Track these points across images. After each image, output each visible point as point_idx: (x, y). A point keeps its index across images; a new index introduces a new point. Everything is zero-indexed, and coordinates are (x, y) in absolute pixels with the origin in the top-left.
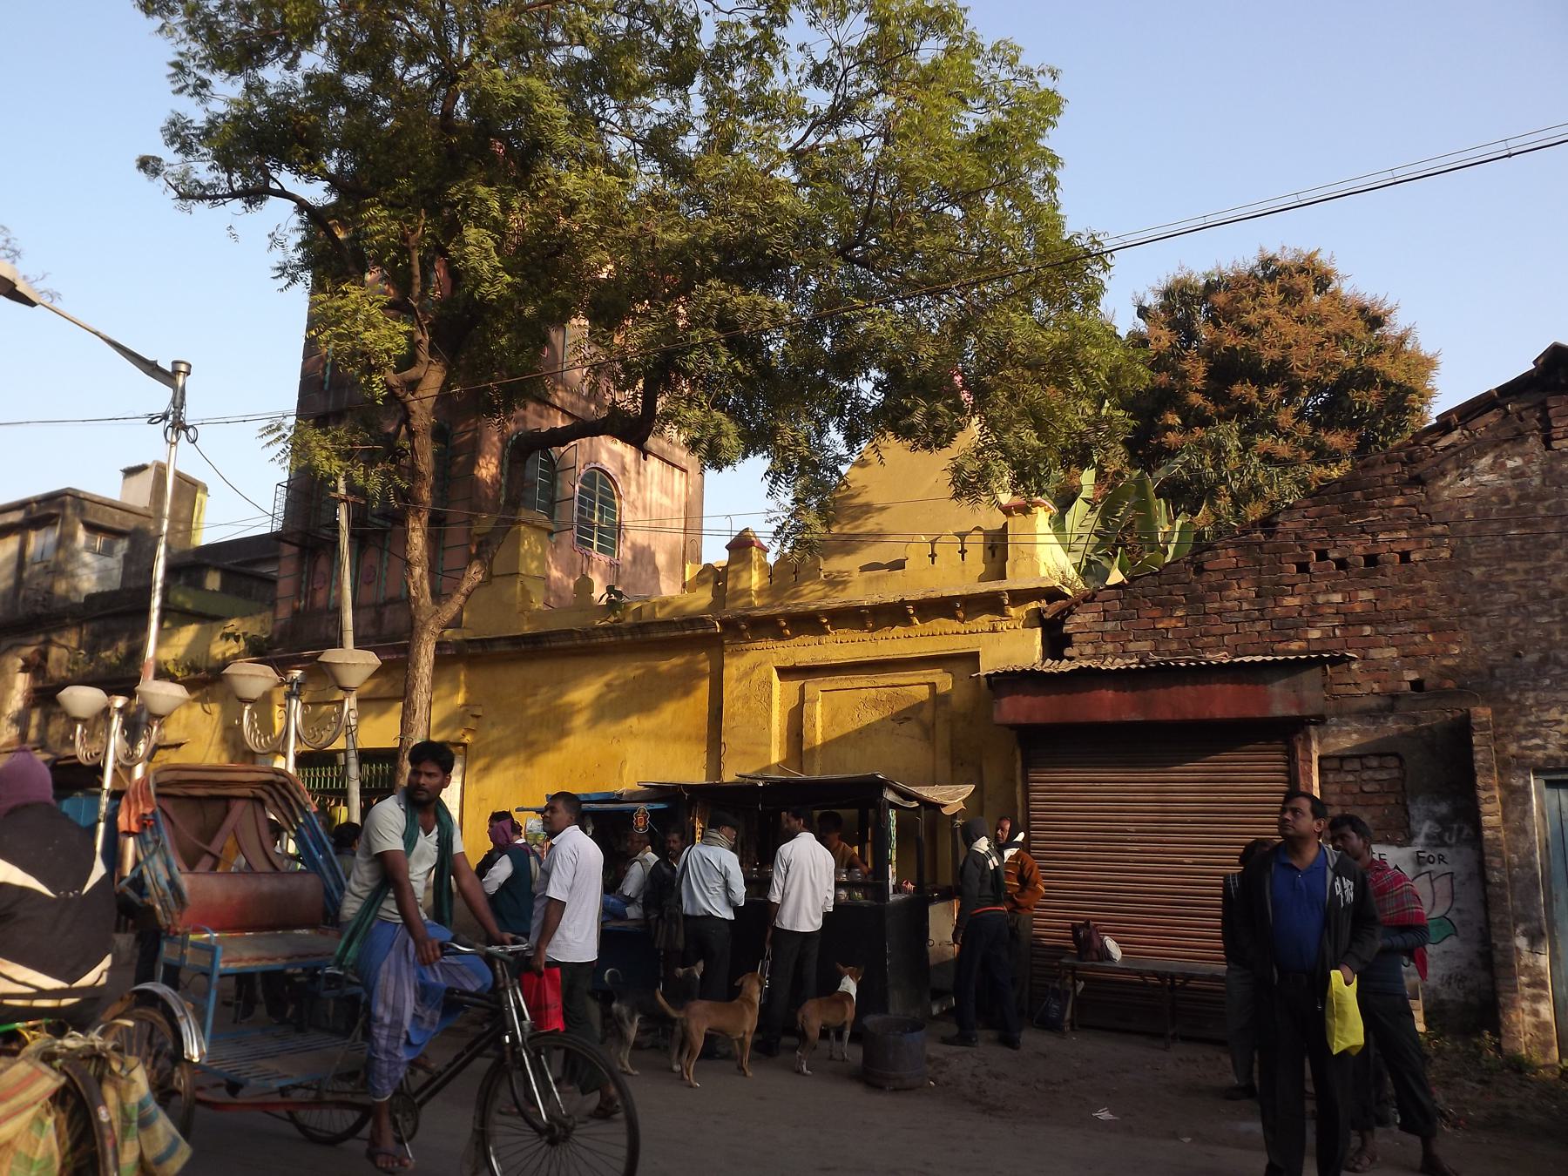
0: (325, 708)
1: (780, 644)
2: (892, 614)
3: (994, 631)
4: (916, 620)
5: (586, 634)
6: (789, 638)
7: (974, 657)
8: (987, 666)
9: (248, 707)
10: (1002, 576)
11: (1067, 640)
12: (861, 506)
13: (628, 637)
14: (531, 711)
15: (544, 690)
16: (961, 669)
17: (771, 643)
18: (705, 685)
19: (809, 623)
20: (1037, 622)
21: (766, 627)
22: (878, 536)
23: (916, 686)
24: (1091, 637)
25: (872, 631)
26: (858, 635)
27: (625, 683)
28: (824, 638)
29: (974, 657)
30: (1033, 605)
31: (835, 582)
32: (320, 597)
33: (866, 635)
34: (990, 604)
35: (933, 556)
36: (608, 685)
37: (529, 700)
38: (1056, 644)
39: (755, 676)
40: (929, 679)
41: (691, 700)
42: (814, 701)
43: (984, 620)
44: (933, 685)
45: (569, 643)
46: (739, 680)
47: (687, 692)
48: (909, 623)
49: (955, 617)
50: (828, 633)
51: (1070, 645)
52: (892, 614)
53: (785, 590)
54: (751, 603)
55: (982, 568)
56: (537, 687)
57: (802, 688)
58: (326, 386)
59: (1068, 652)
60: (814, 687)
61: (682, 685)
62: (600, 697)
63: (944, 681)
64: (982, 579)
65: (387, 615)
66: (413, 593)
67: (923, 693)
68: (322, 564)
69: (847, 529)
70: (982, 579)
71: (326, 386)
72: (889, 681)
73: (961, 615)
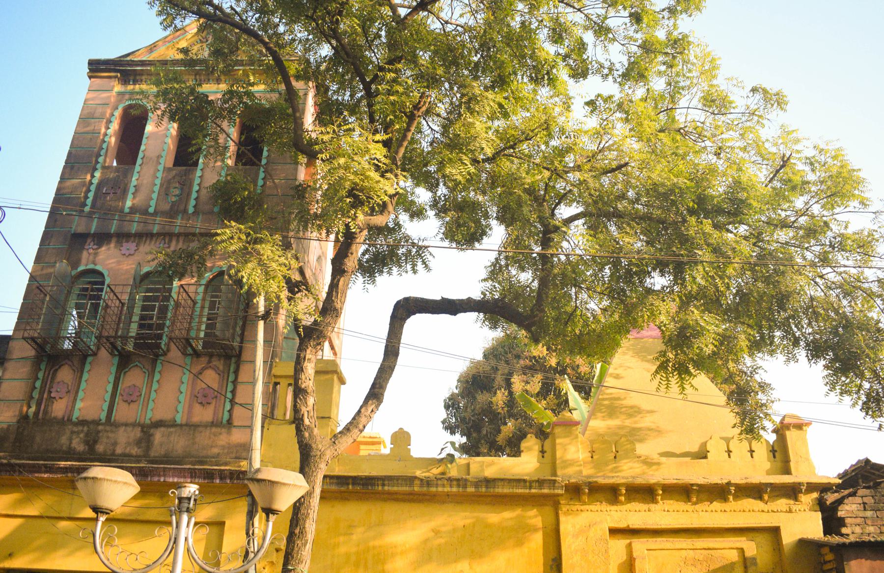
0: (63, 524)
1: (614, 508)
2: (719, 492)
3: (790, 511)
4: (731, 498)
5: (427, 482)
6: (622, 503)
7: (775, 532)
8: (788, 538)
9: (102, 519)
10: (787, 471)
11: (841, 522)
12: (632, 407)
13: (471, 490)
14: (342, 550)
15: (360, 530)
16: (763, 539)
17: (605, 506)
18: (537, 541)
19: (645, 493)
20: (818, 508)
21: (612, 493)
22: (658, 432)
23: (728, 550)
24: (858, 521)
25: (696, 504)
26: (681, 506)
27: (454, 530)
28: (653, 506)
29: (775, 532)
30: (815, 495)
31: (648, 462)
32: (59, 409)
33: (688, 506)
34: (792, 492)
35: (729, 452)
36: (436, 532)
37: (342, 539)
38: (832, 522)
39: (591, 534)
40: (738, 545)
41: (525, 549)
42: (643, 558)
43: (783, 503)
44: (742, 551)
45: (406, 489)
46: (576, 536)
47: (520, 543)
48: (726, 500)
49: (760, 498)
50: (657, 503)
51: (844, 525)
52: (719, 492)
53: (607, 464)
54: (581, 472)
55: (767, 465)
56: (351, 526)
57: (630, 544)
58: (87, 209)
59: (844, 530)
60: (640, 545)
61: (518, 534)
62: (426, 541)
63: (751, 547)
64: (769, 473)
65: (158, 436)
66: (307, 422)
67: (734, 556)
68: (65, 374)
69: (628, 423)
70: (769, 473)
71: (87, 209)
72: (706, 547)
73: (766, 497)
